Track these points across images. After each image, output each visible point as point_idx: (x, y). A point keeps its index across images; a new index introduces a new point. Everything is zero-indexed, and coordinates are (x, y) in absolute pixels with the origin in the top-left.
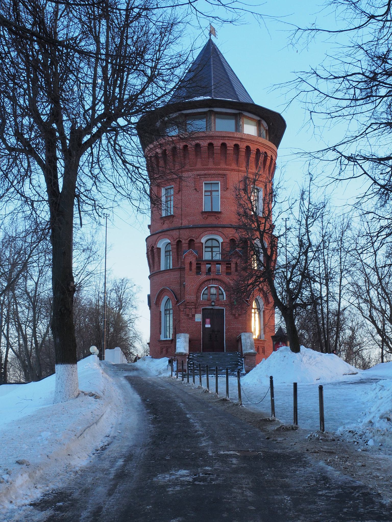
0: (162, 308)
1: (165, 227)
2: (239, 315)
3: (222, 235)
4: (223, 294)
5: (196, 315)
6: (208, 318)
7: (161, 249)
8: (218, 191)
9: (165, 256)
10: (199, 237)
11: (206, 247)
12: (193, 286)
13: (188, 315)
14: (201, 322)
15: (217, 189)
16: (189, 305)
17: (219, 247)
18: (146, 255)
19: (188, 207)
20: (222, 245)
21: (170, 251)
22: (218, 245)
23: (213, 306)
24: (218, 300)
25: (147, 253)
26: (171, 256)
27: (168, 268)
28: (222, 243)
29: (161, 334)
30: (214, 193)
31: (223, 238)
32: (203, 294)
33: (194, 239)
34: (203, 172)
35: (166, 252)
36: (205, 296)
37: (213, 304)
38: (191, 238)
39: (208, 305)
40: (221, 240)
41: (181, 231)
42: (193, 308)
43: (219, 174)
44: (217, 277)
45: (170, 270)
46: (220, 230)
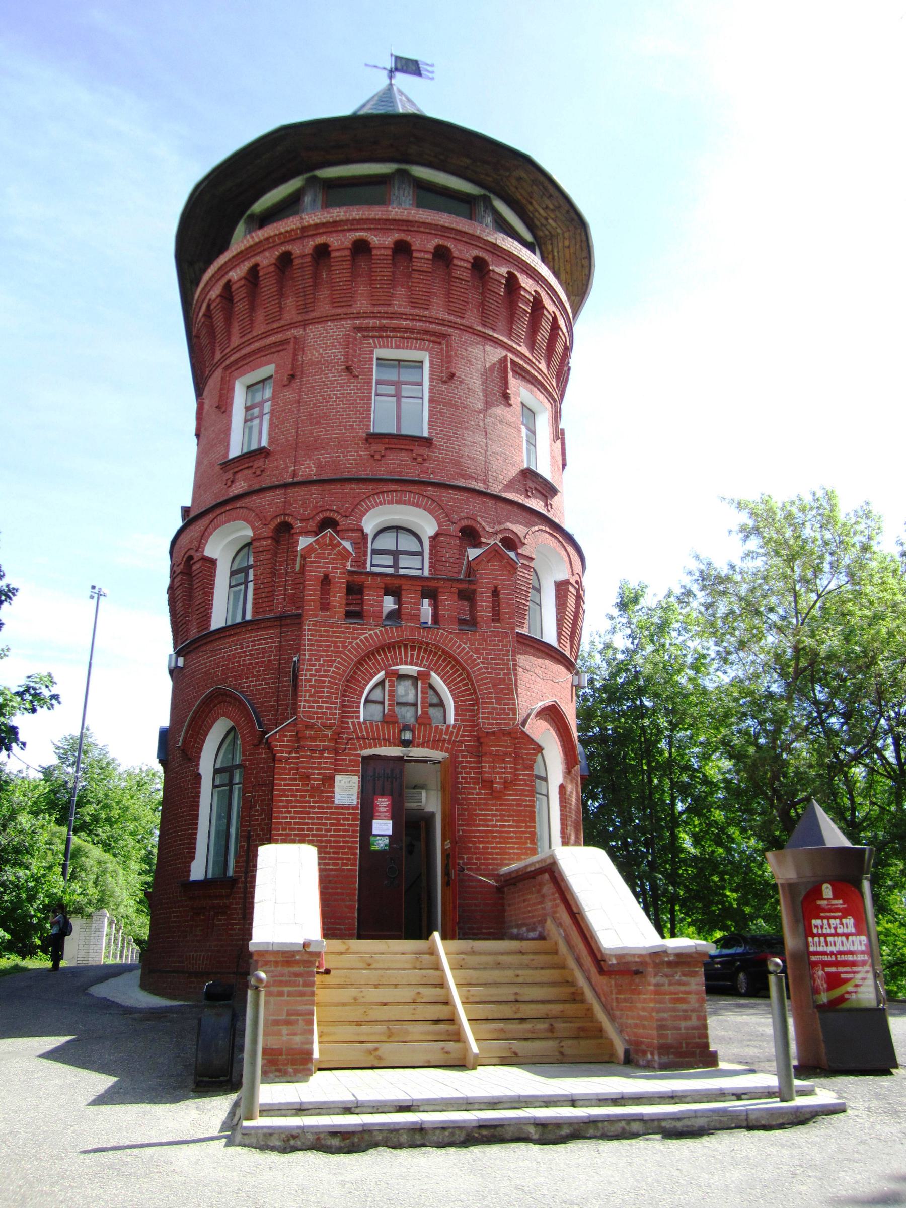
0: (206, 765)
1: (240, 487)
2: (507, 784)
3: (436, 509)
4: (441, 704)
5: (338, 778)
6: (383, 795)
7: (218, 563)
8: (421, 384)
9: (230, 587)
10: (357, 509)
11: (375, 552)
12: (330, 663)
13: (307, 777)
14: (355, 808)
15: (416, 379)
16: (313, 739)
17: (421, 554)
18: (166, 597)
19: (318, 423)
20: (432, 547)
21: (245, 570)
22: (416, 547)
23: (406, 744)
24: (423, 721)
25: (171, 590)
26: (251, 586)
27: (239, 619)
28: (434, 538)
29: (193, 858)
30: (406, 390)
31: (437, 519)
32: (367, 701)
33: (338, 518)
34: (372, 322)
35: (233, 573)
36: (376, 712)
37: (407, 736)
38: (328, 514)
39: (387, 742)
40: (428, 527)
41: (291, 492)
42: (326, 748)
43: (426, 332)
44: (424, 636)
45: (245, 623)
46: (430, 492)
